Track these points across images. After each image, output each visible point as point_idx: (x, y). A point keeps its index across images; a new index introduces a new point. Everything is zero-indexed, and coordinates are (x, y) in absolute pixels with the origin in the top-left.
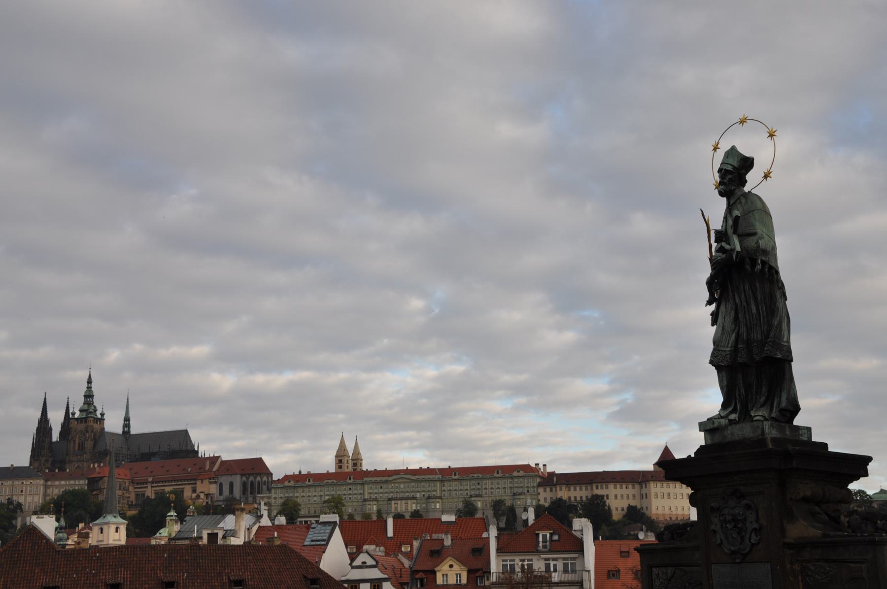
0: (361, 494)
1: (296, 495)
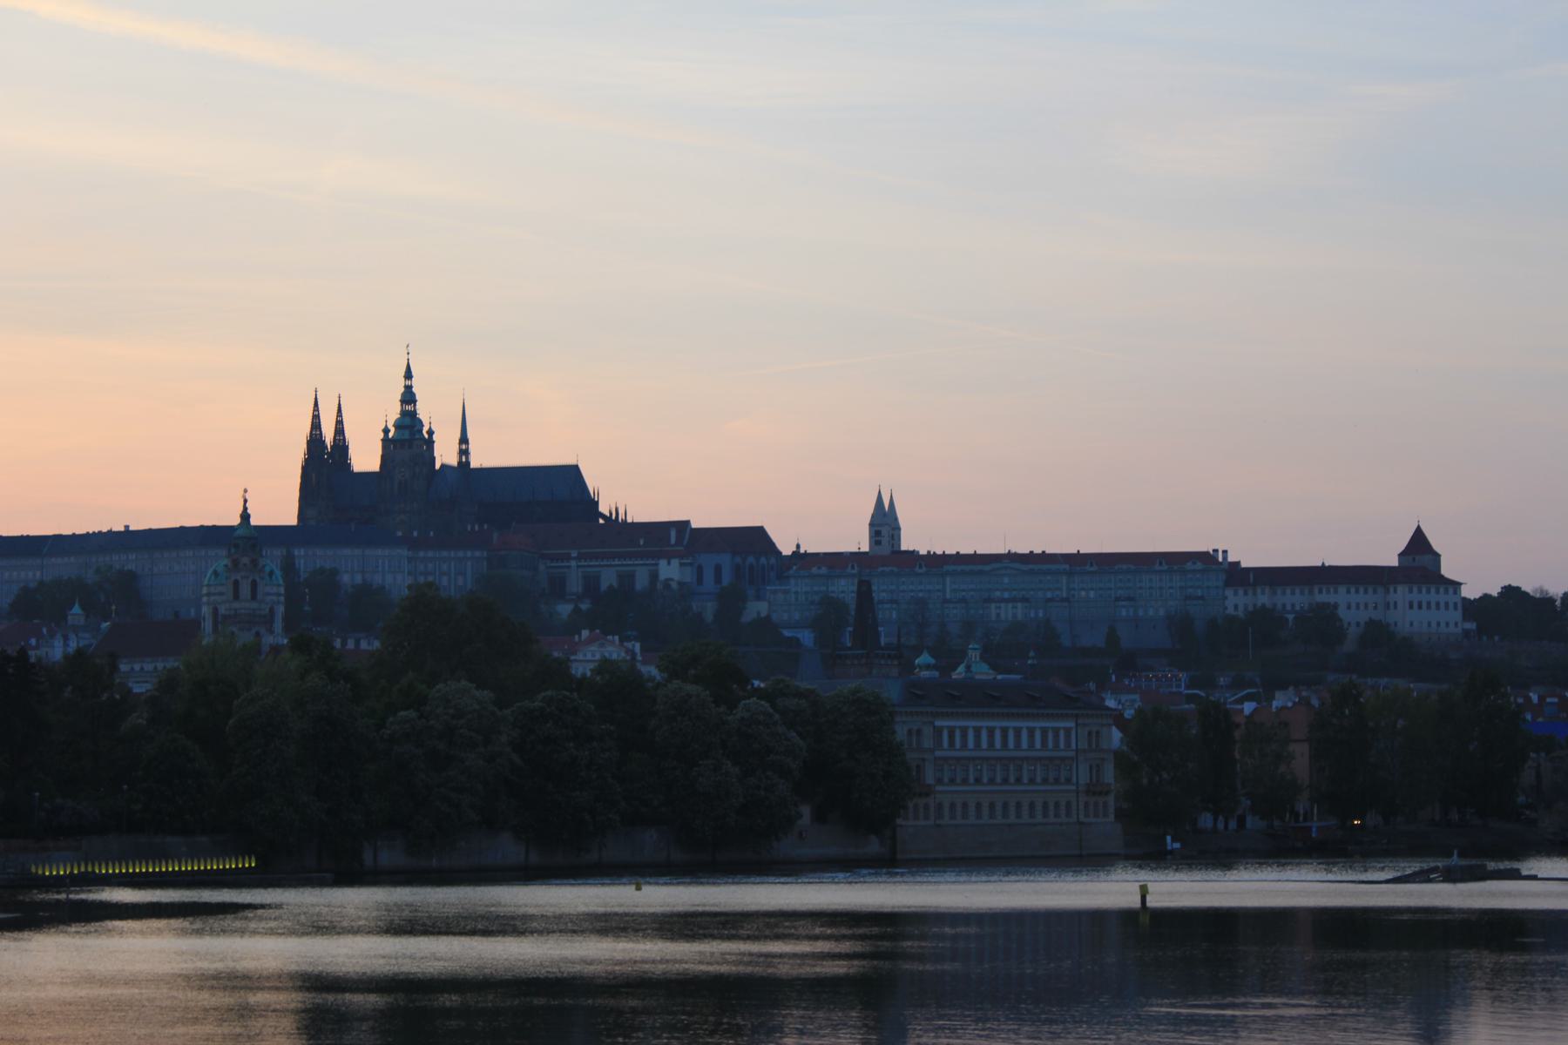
0: (939, 590)
1: (831, 588)
